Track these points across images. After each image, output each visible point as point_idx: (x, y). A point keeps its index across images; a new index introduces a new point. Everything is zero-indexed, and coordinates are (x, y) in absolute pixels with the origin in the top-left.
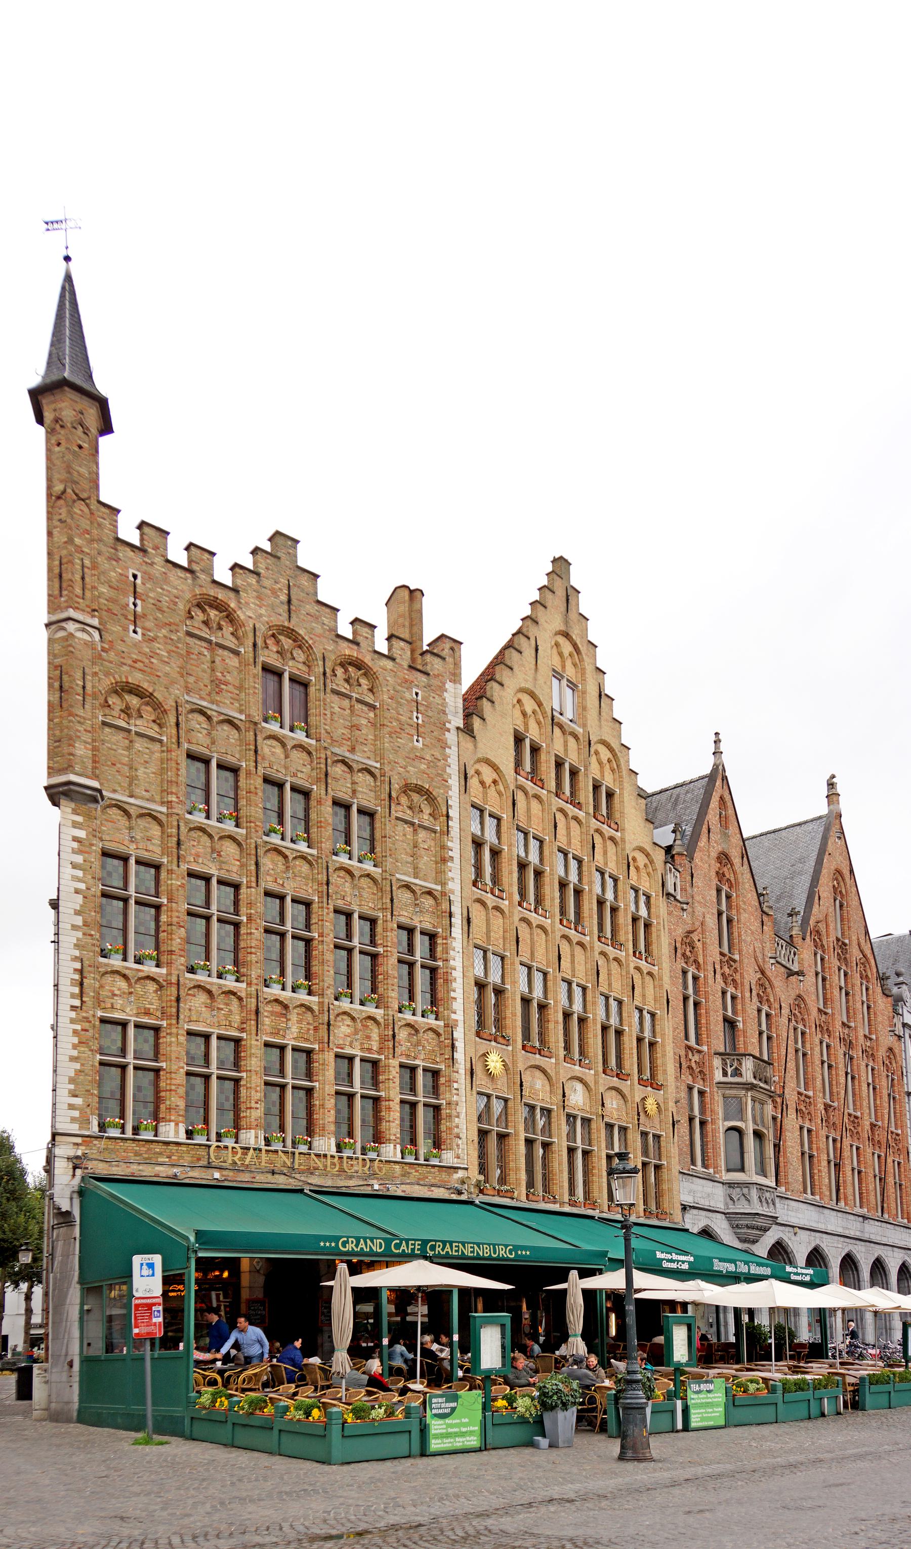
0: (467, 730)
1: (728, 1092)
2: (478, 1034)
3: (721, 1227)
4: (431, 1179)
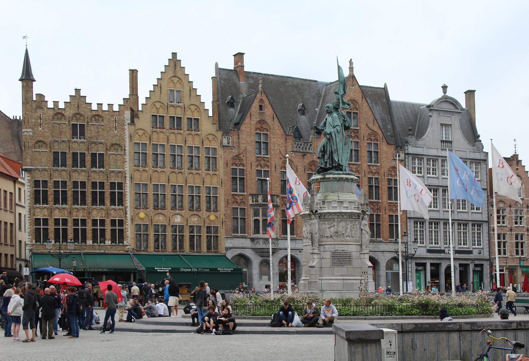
0: (132, 122)
3: (249, 253)
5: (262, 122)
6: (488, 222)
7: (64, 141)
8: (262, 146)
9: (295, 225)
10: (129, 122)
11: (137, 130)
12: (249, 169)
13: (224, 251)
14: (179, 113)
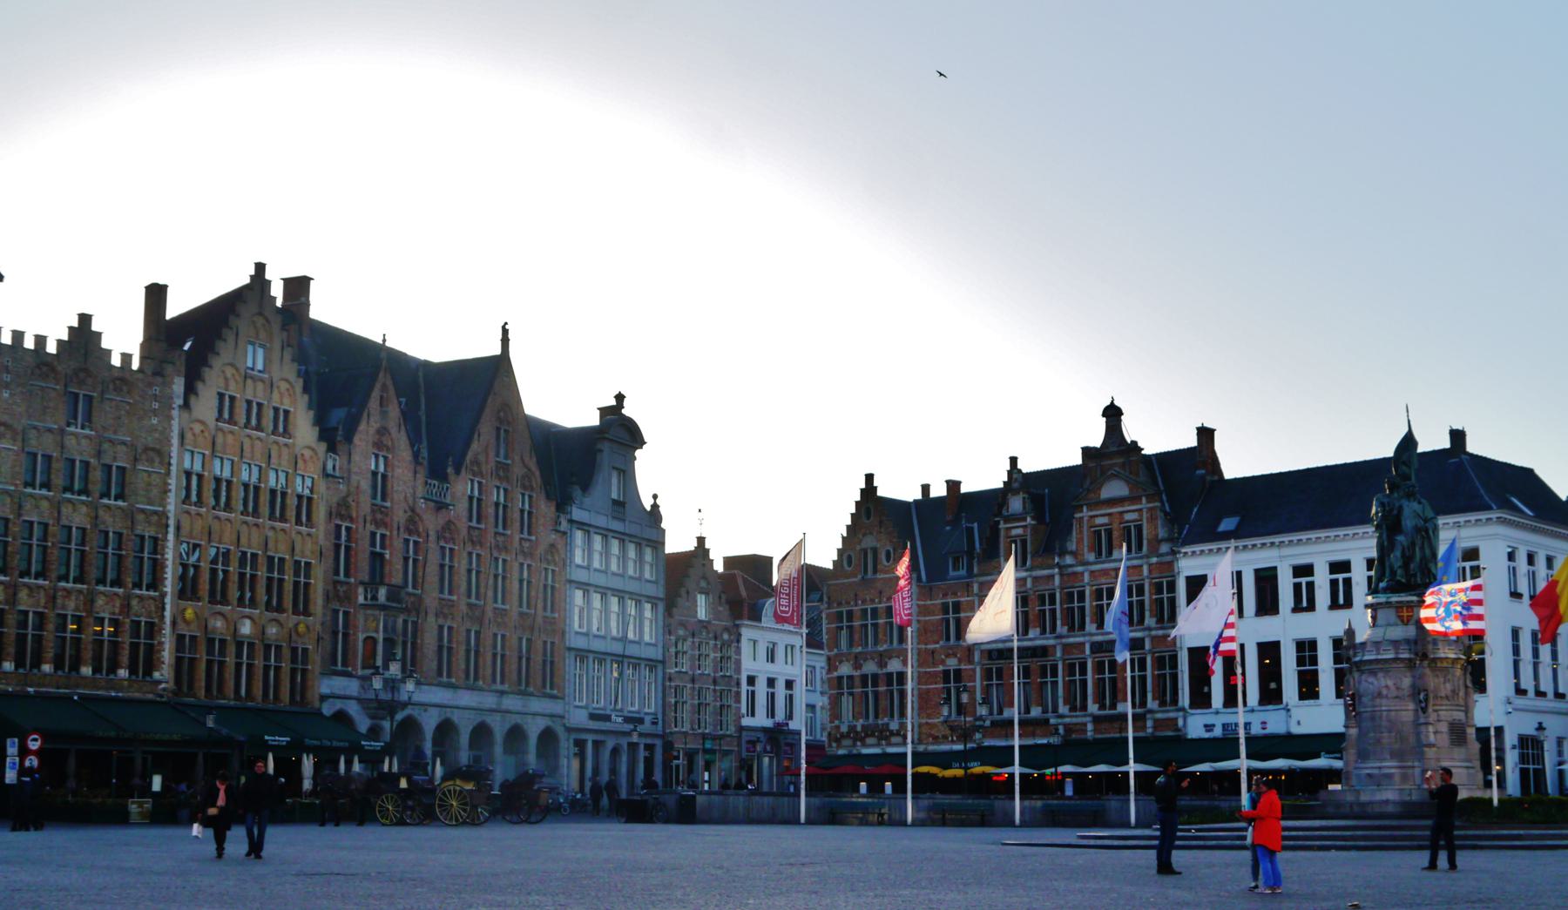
0: (186, 405)
2: (180, 598)
3: (353, 709)
6: (663, 662)
7: (50, 430)
10: (180, 402)
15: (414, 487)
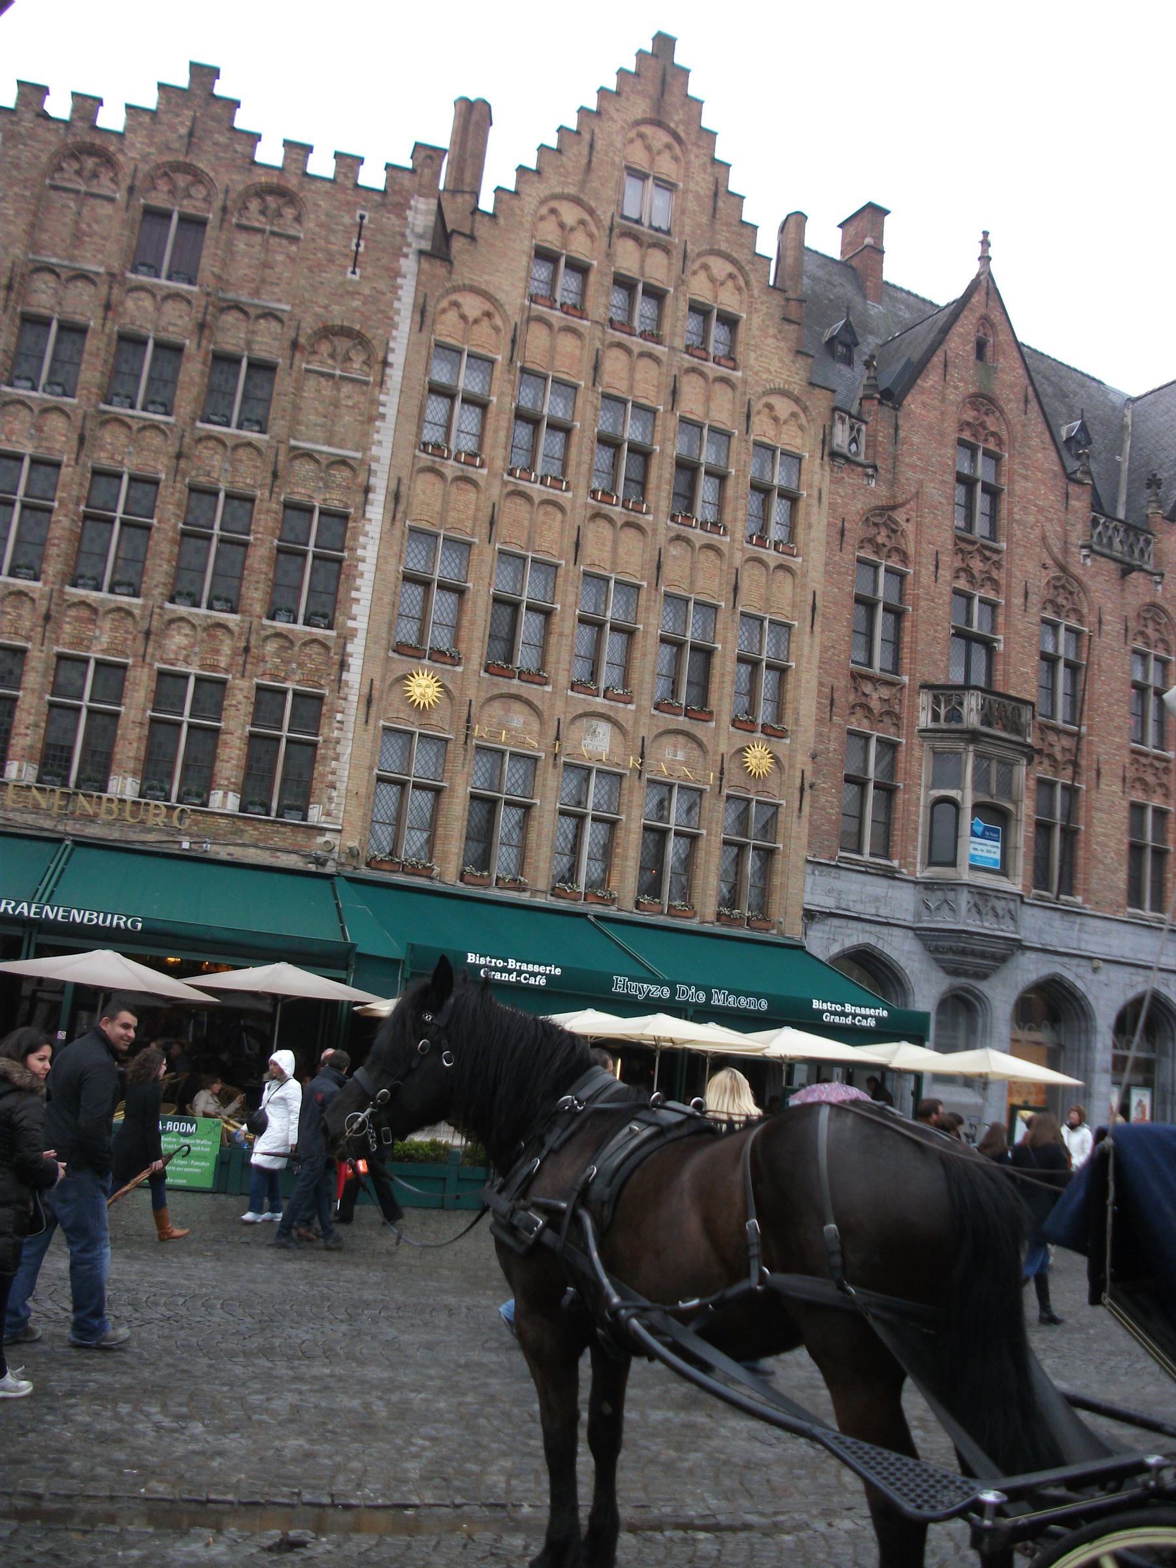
1: (938, 744)
3: (902, 951)
4: (277, 841)
5: (983, 401)
8: (982, 494)
9: (1081, 853)
11: (456, 289)
12: (926, 578)
13: (792, 928)
14: (657, 269)
15: (1064, 524)
